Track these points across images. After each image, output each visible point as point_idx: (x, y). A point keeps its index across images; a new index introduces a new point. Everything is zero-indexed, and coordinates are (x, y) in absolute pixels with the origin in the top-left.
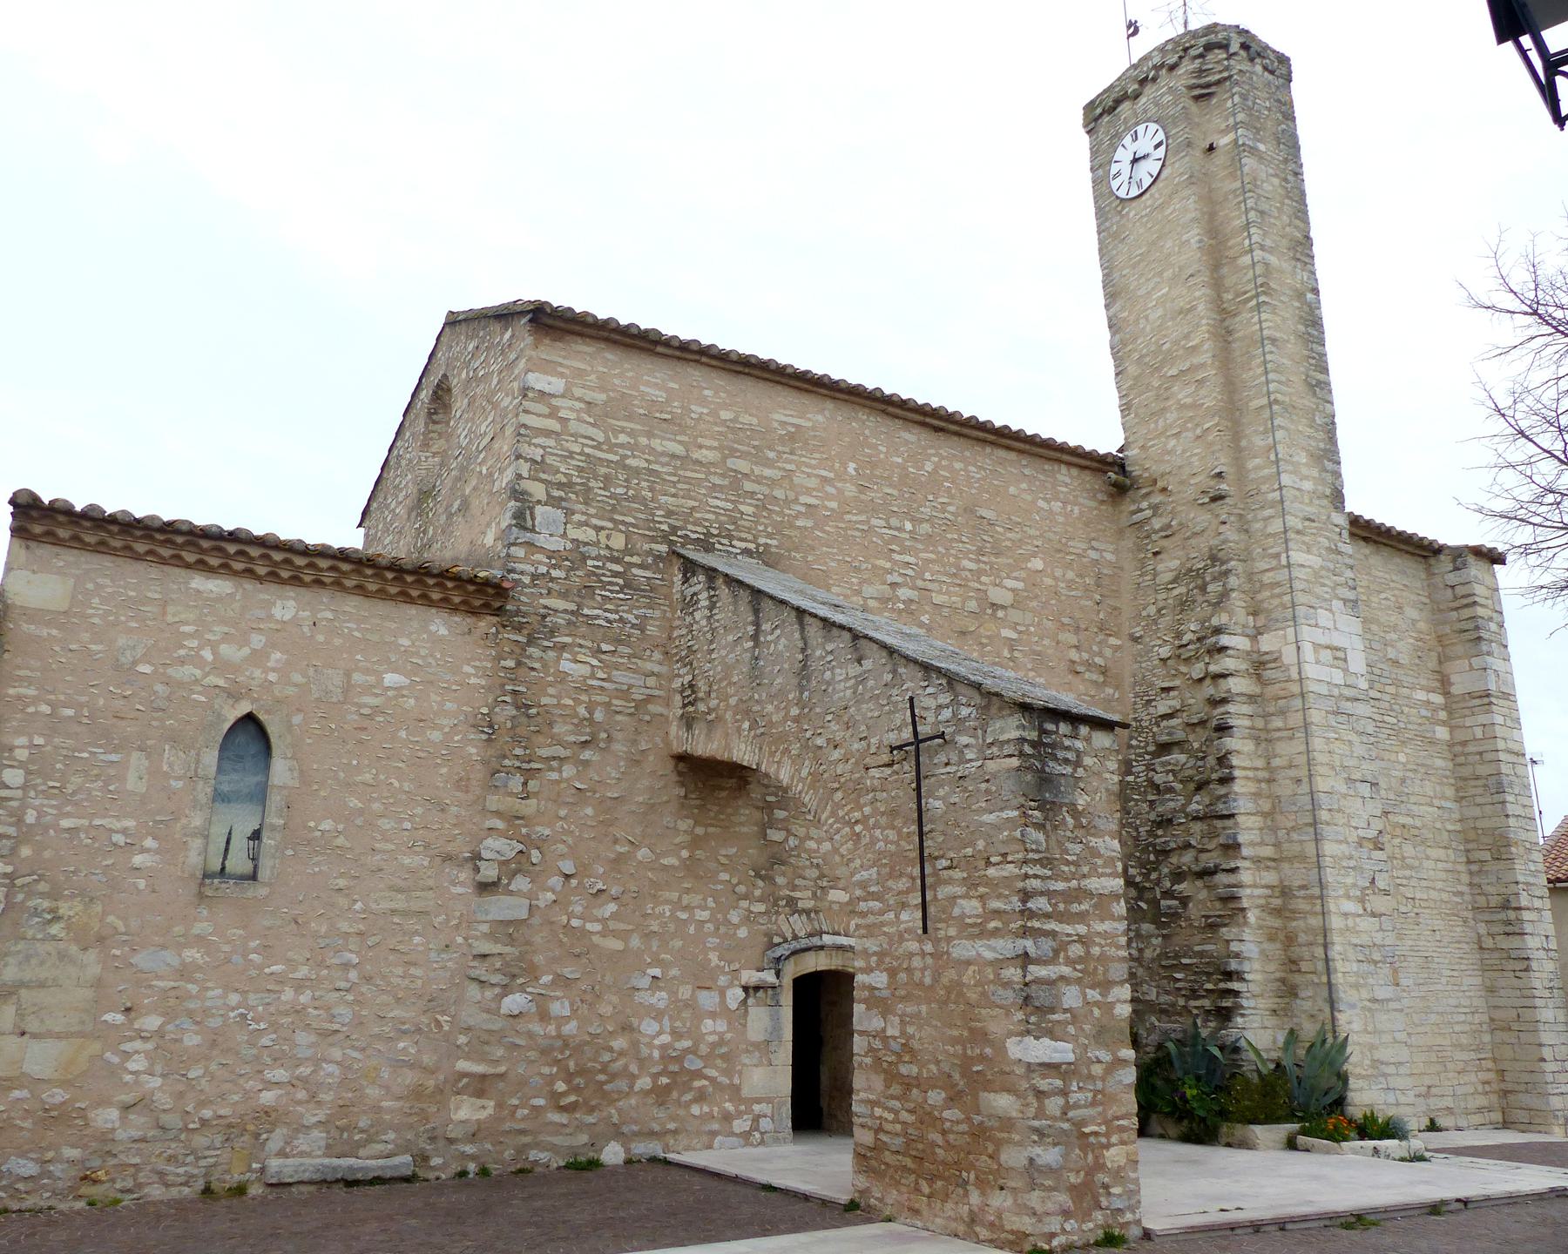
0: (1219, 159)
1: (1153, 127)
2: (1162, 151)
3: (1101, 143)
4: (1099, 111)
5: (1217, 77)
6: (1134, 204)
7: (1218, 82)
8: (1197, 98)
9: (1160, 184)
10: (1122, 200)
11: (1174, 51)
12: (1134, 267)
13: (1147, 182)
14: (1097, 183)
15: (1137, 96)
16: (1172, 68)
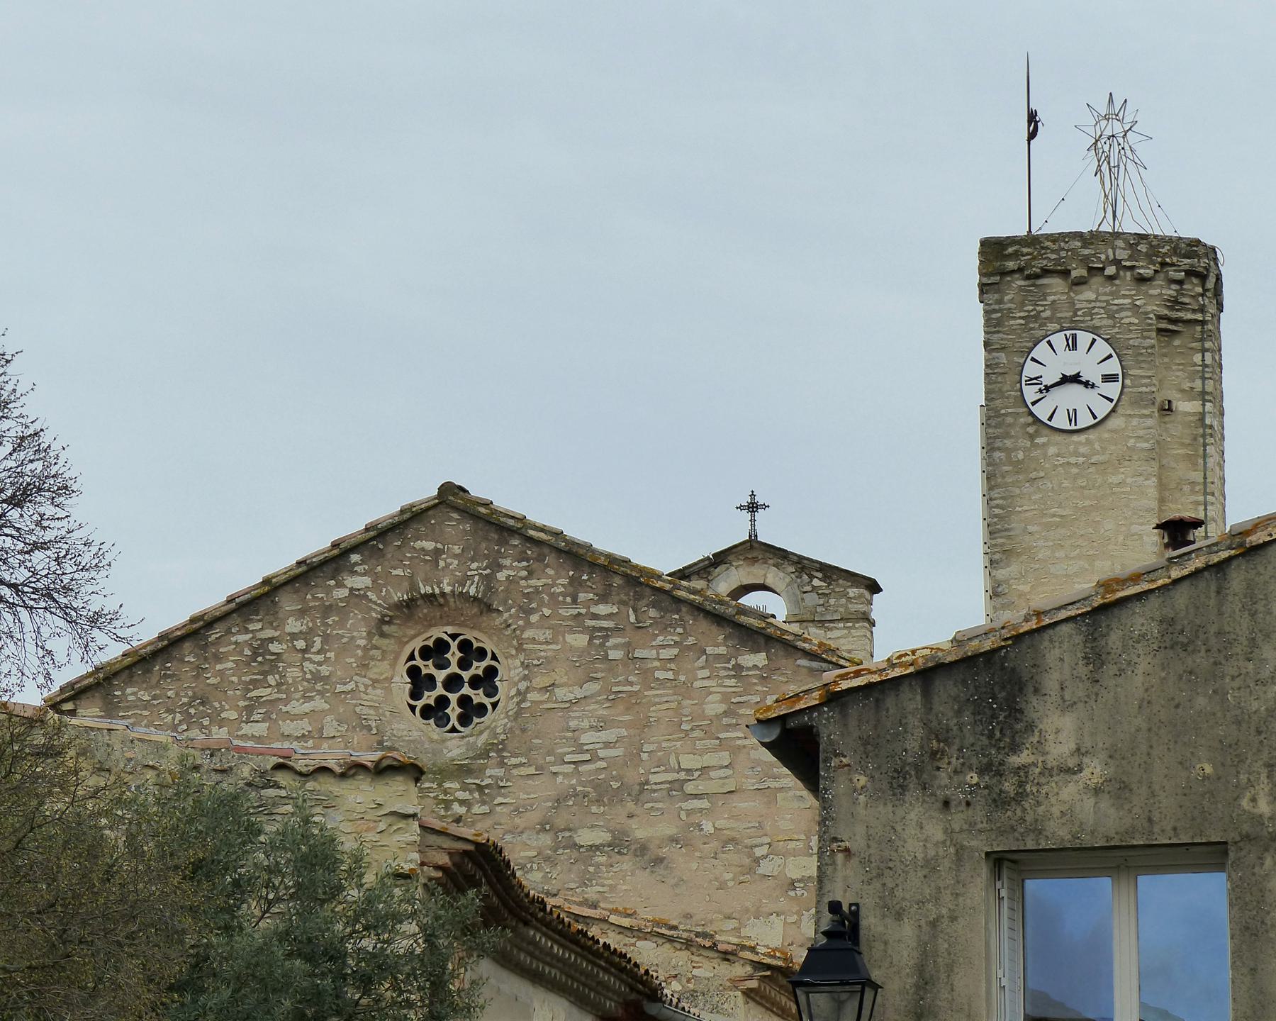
0: (1176, 429)
1: (1103, 348)
2: (1113, 390)
3: (1008, 314)
4: (1011, 265)
5: (1190, 316)
6: (1059, 438)
7: (1189, 321)
8: (1160, 331)
9: (1103, 433)
10: (1037, 420)
11: (1149, 256)
12: (1048, 527)
13: (1085, 420)
14: (992, 371)
15: (1080, 282)
16: (1142, 280)
